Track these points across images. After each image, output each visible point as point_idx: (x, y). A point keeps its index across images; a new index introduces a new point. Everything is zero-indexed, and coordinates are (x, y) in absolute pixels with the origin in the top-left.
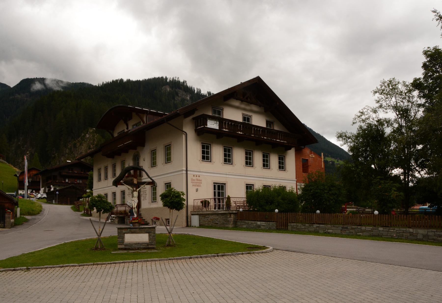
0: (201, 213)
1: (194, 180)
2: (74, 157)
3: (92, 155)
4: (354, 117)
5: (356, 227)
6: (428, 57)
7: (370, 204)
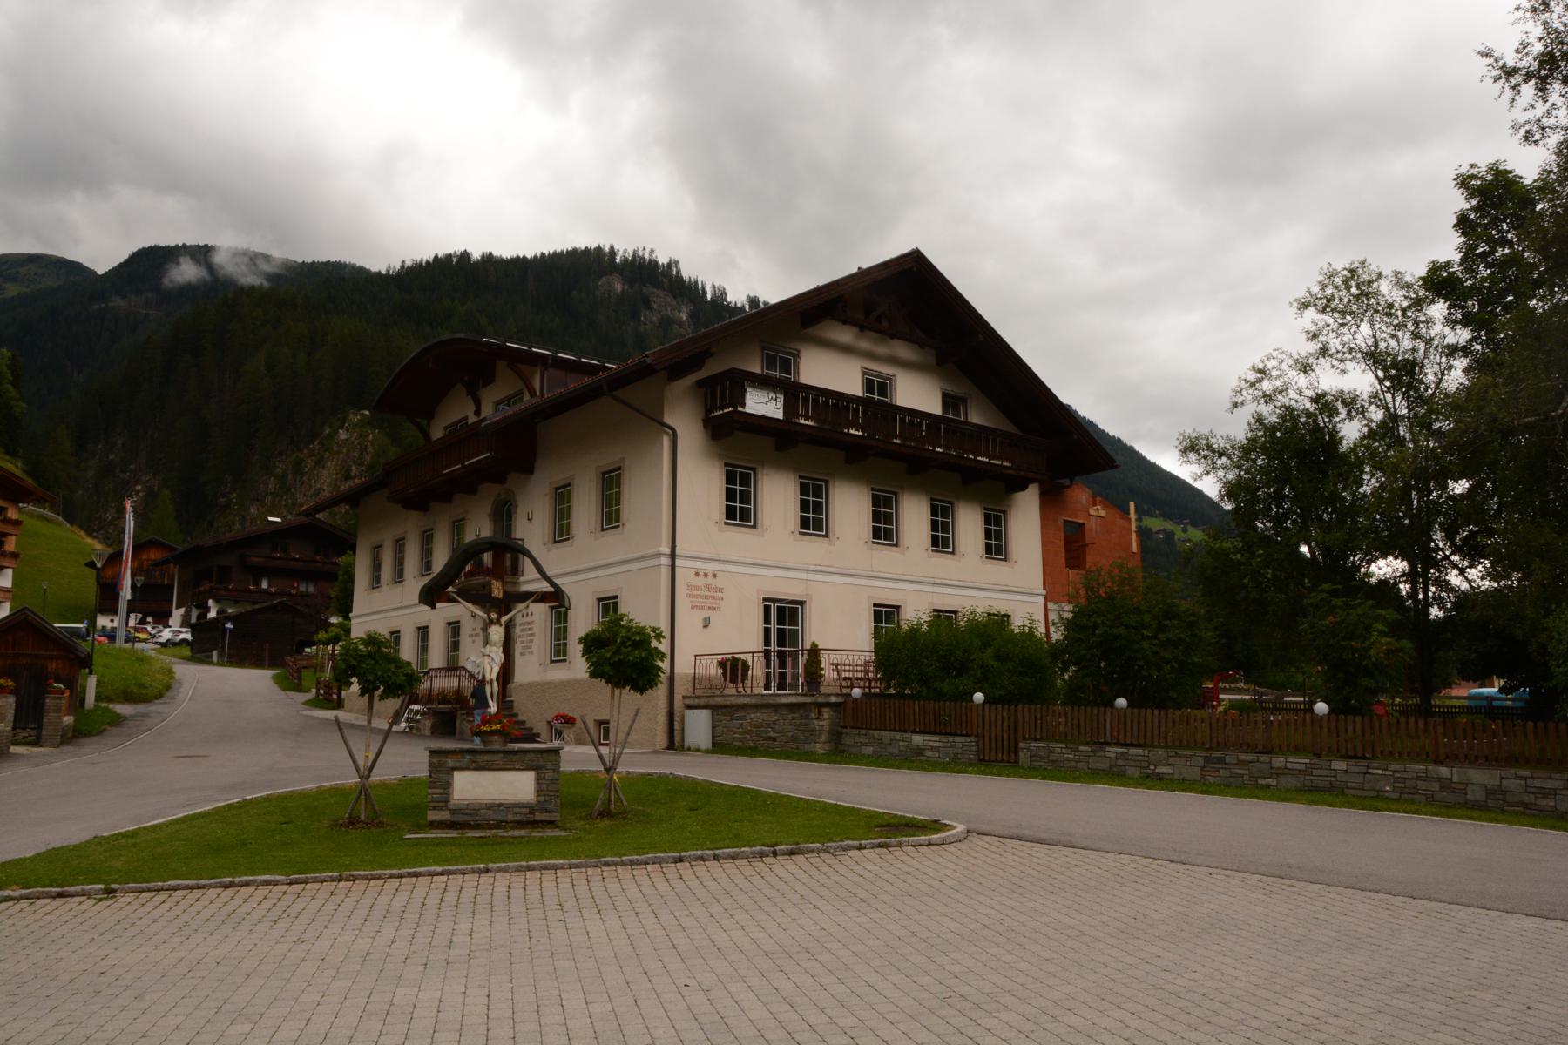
0: (719, 700)
1: (698, 588)
2: (294, 504)
3: (354, 498)
4: (1234, 383)
5: (1253, 757)
6: (1471, 195)
7: (1300, 678)
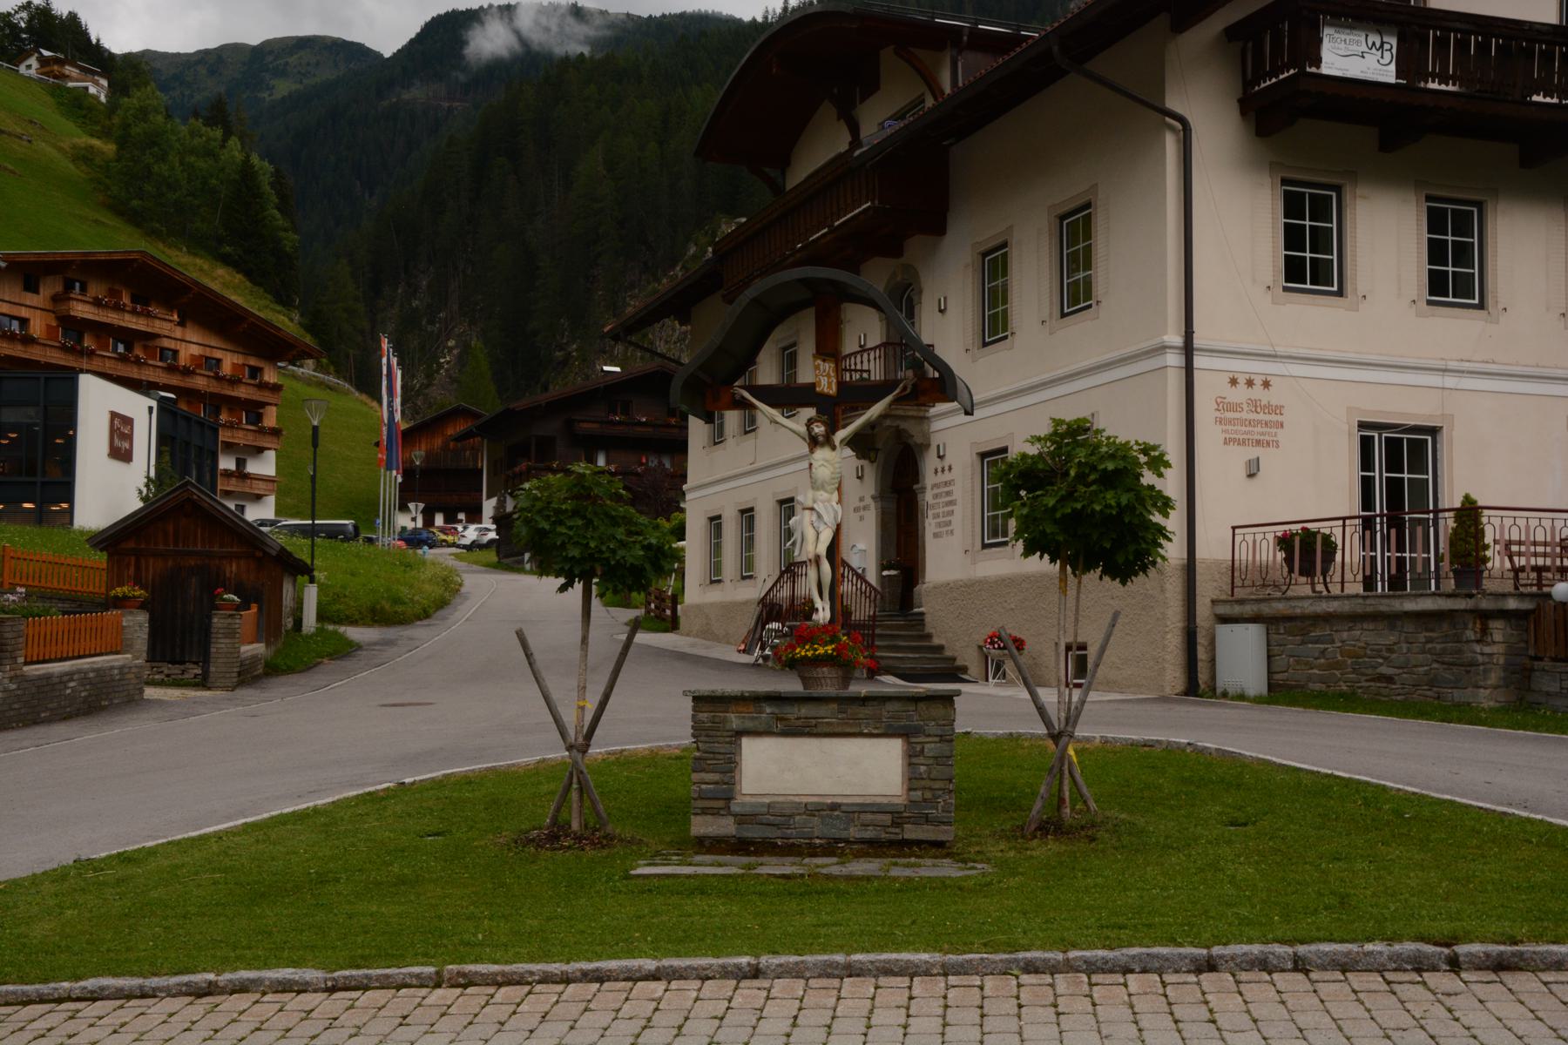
0: (1280, 607)
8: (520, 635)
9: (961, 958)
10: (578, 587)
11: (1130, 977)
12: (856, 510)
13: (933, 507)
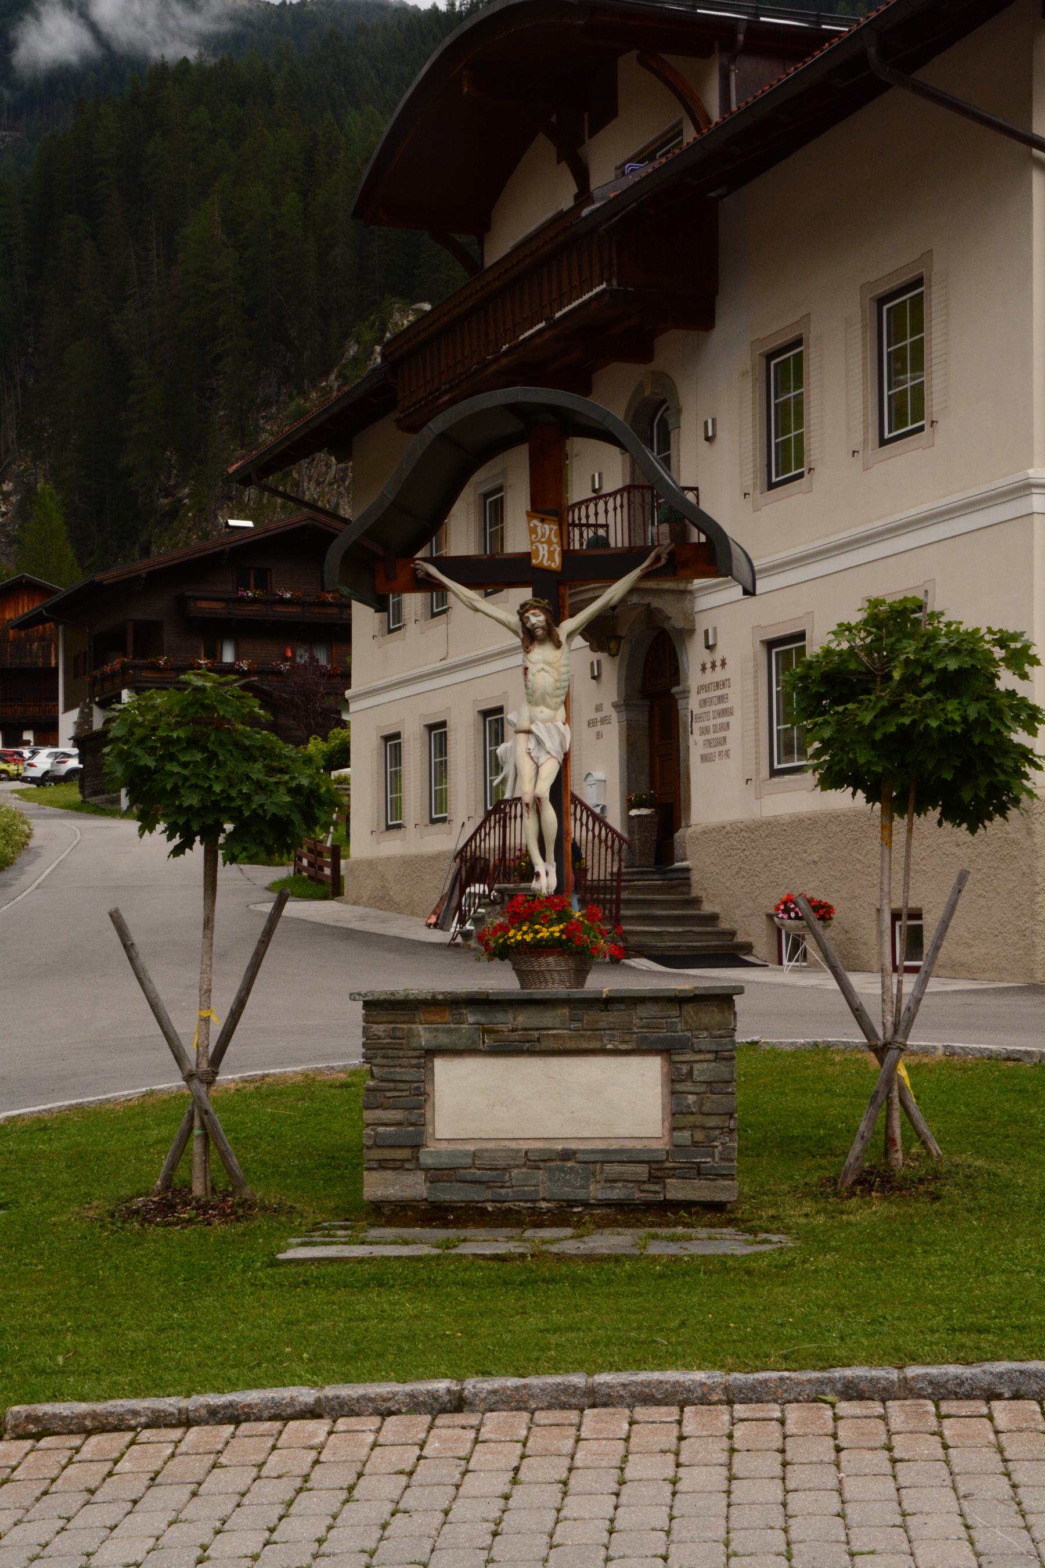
8: (116, 919)
9: (751, 1377)
10: (199, 848)
11: (995, 1404)
12: (591, 723)
13: (700, 718)
